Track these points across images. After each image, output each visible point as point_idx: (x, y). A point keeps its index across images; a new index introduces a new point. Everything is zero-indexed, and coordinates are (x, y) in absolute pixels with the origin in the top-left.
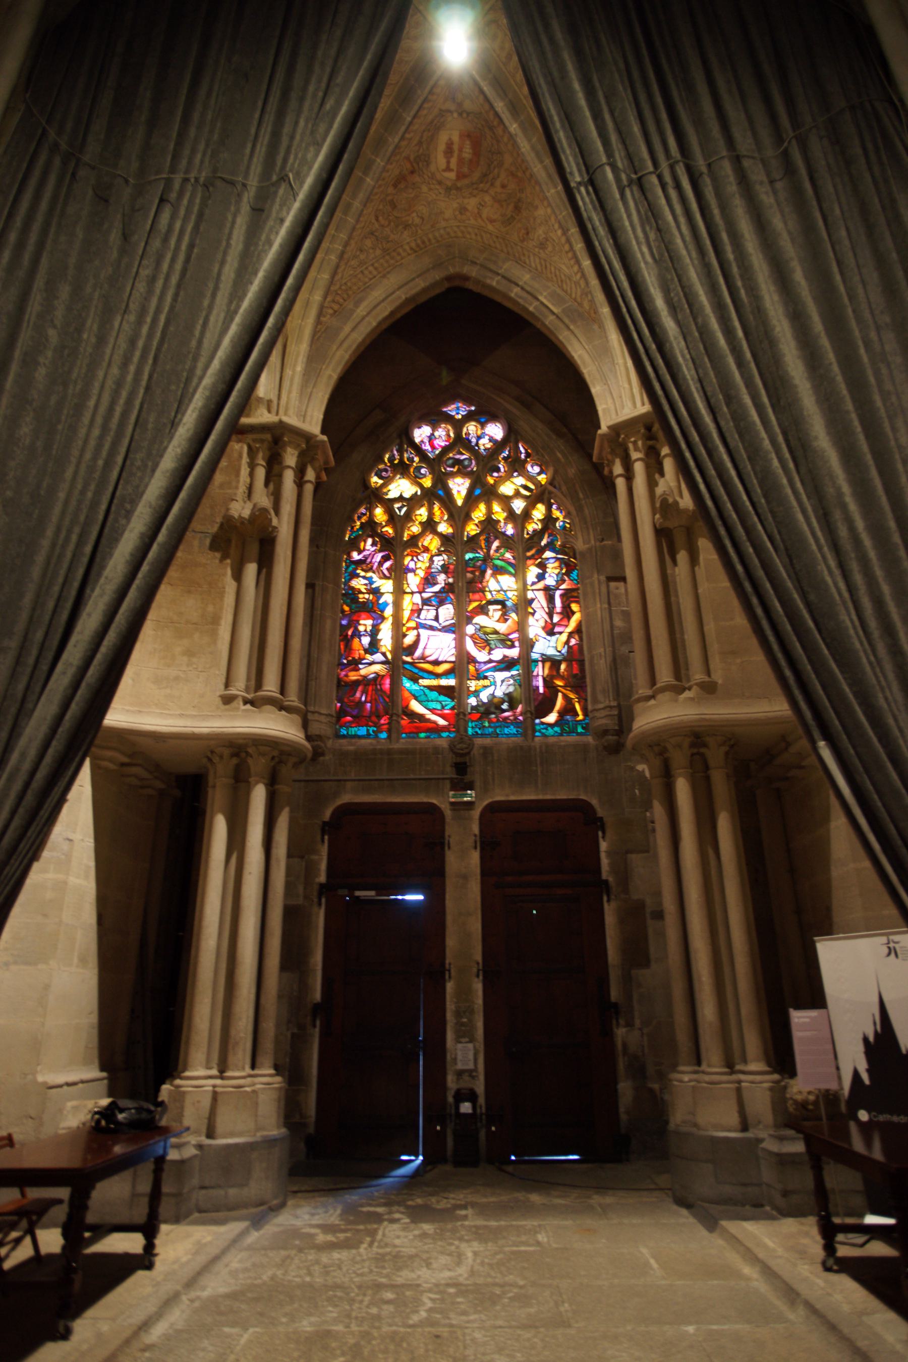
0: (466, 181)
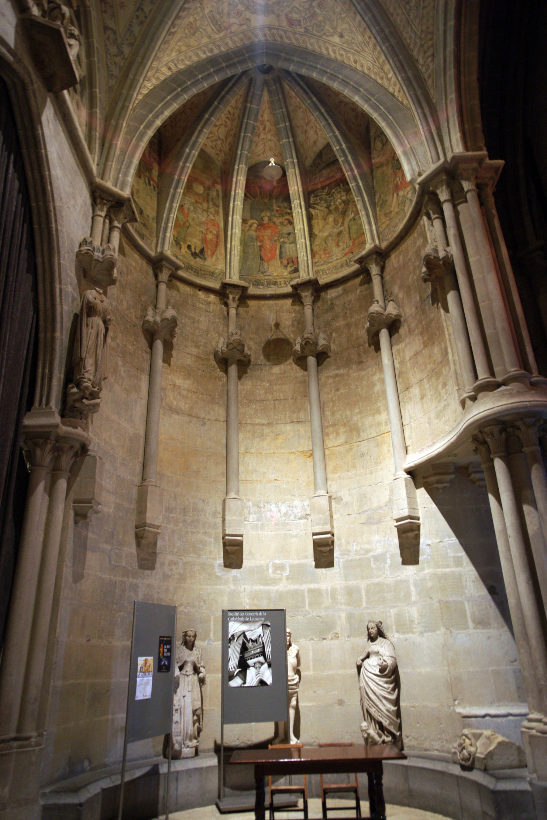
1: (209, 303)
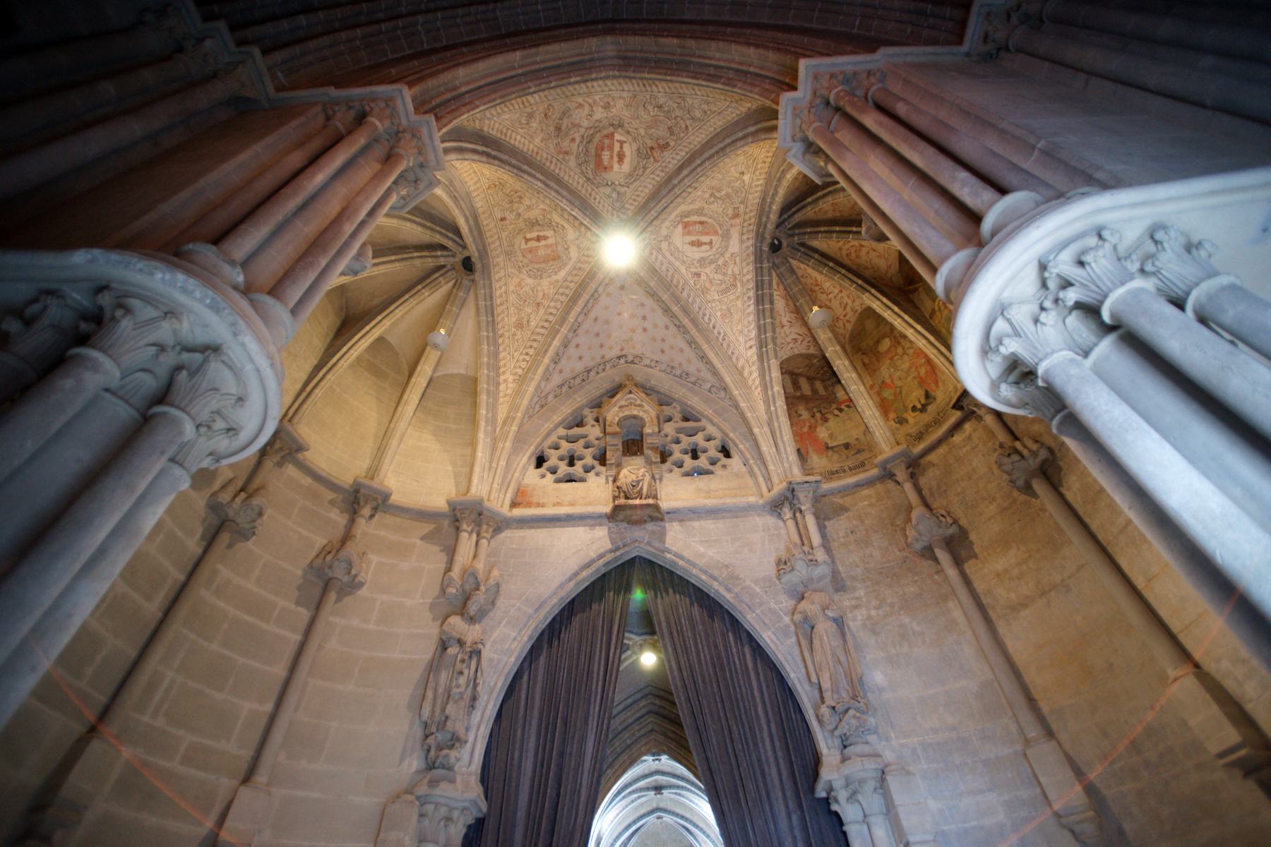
0: (605, 132)
1: (969, 438)
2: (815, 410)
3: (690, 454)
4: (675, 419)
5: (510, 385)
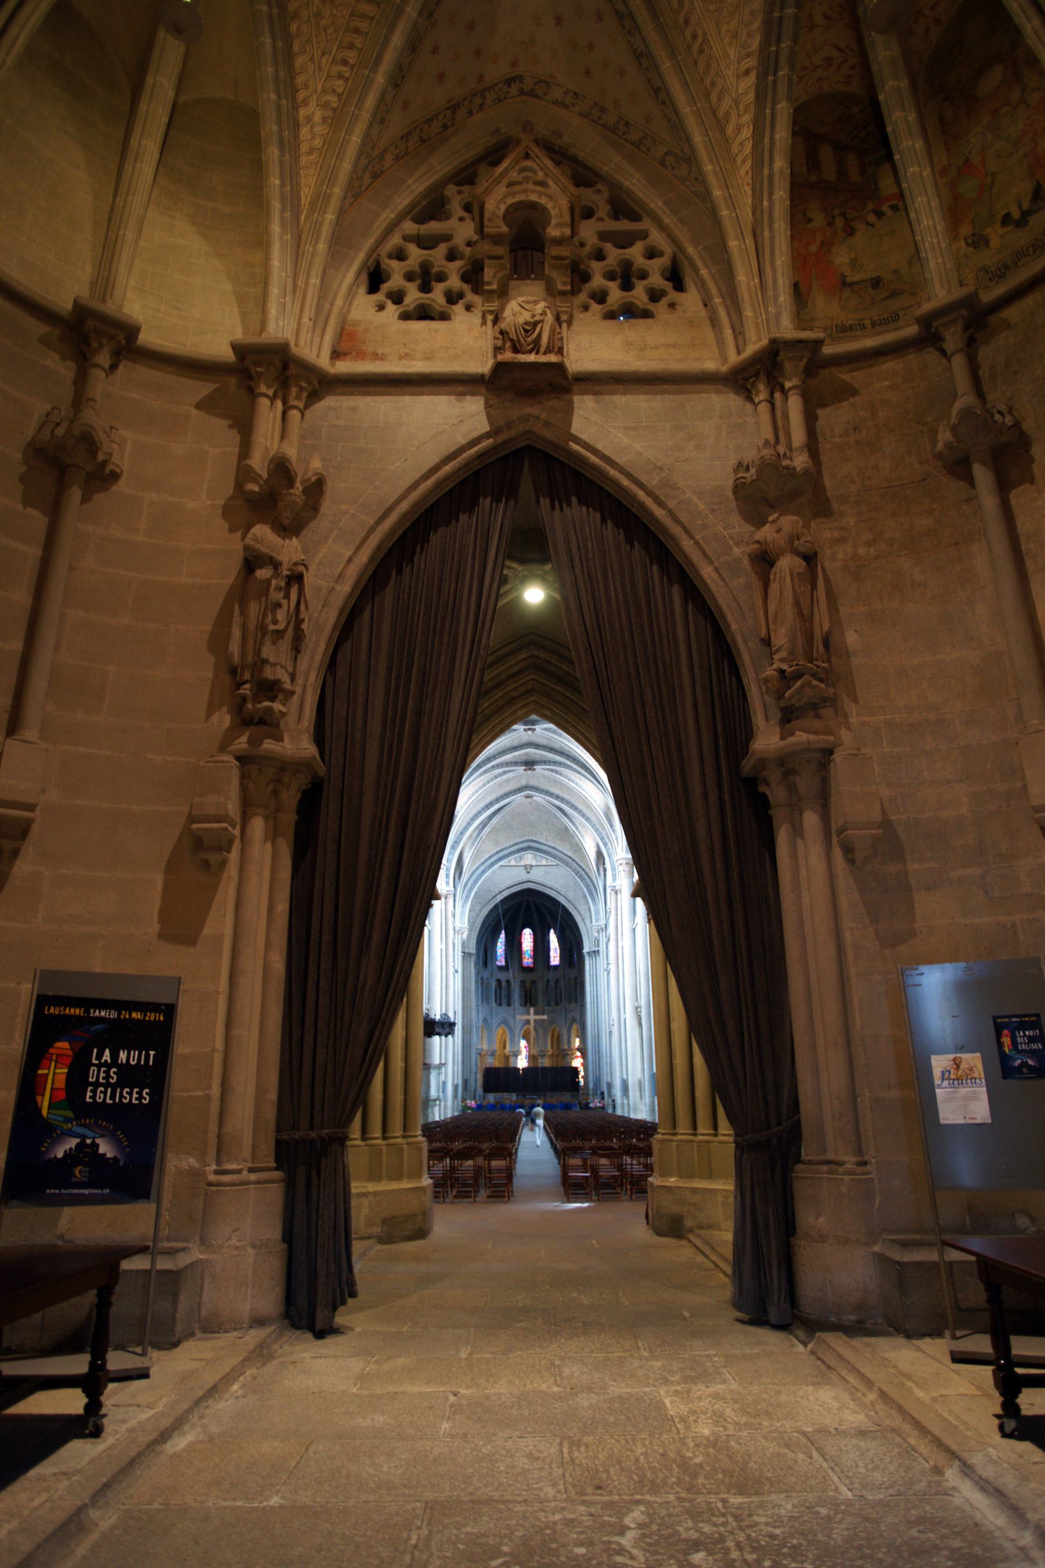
2: (836, 212)
3: (619, 281)
4: (600, 214)
5: (318, 129)
